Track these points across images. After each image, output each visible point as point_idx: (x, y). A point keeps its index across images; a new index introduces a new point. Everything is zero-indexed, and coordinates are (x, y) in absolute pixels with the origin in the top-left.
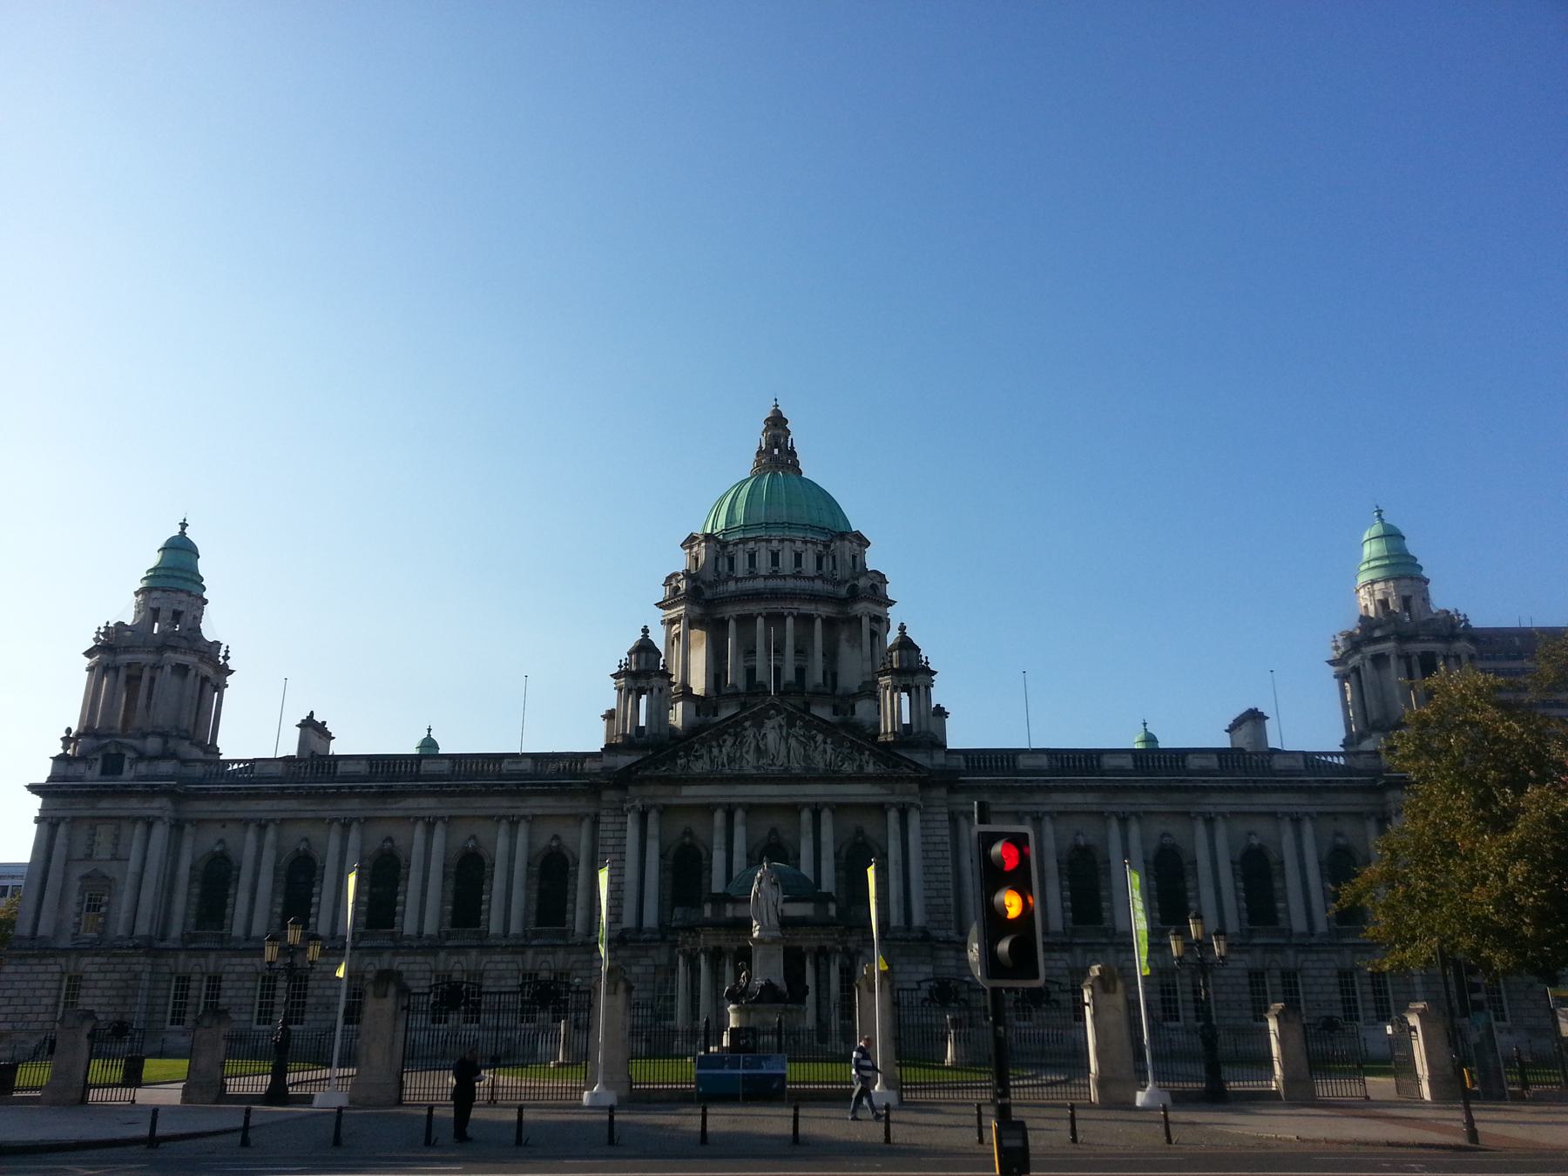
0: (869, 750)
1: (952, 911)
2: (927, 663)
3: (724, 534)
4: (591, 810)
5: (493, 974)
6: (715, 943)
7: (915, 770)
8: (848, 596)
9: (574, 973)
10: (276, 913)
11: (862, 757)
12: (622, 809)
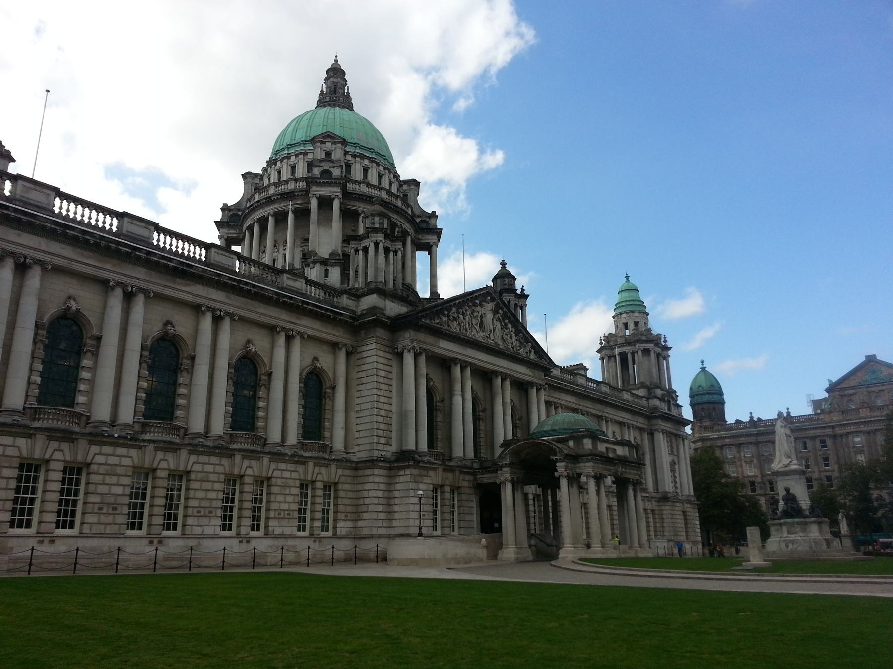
5: (279, 482)
9: (340, 486)
10: (35, 383)
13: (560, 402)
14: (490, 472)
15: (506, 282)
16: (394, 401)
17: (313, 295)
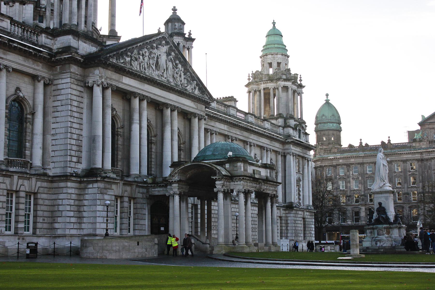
9: (39, 196)
13: (215, 129)
14: (160, 187)
15: (177, 27)
16: (85, 127)
17: (16, 33)
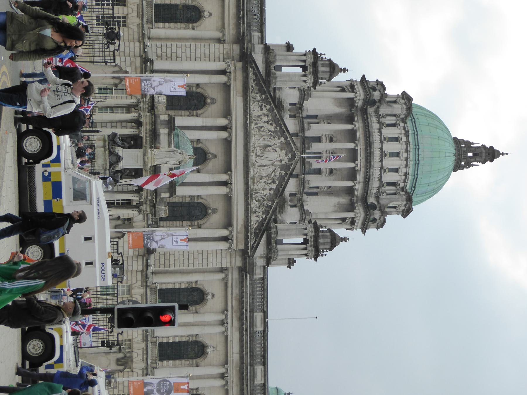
0: (266, 218)
1: (166, 268)
2: (322, 255)
3: (412, 120)
4: (227, 38)
6: (144, 123)
7: (253, 246)
8: (368, 203)
11: (261, 213)
12: (228, 58)
